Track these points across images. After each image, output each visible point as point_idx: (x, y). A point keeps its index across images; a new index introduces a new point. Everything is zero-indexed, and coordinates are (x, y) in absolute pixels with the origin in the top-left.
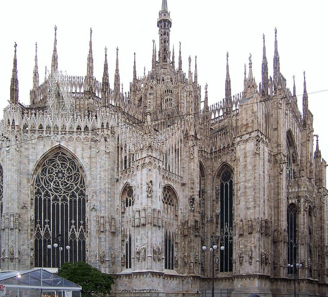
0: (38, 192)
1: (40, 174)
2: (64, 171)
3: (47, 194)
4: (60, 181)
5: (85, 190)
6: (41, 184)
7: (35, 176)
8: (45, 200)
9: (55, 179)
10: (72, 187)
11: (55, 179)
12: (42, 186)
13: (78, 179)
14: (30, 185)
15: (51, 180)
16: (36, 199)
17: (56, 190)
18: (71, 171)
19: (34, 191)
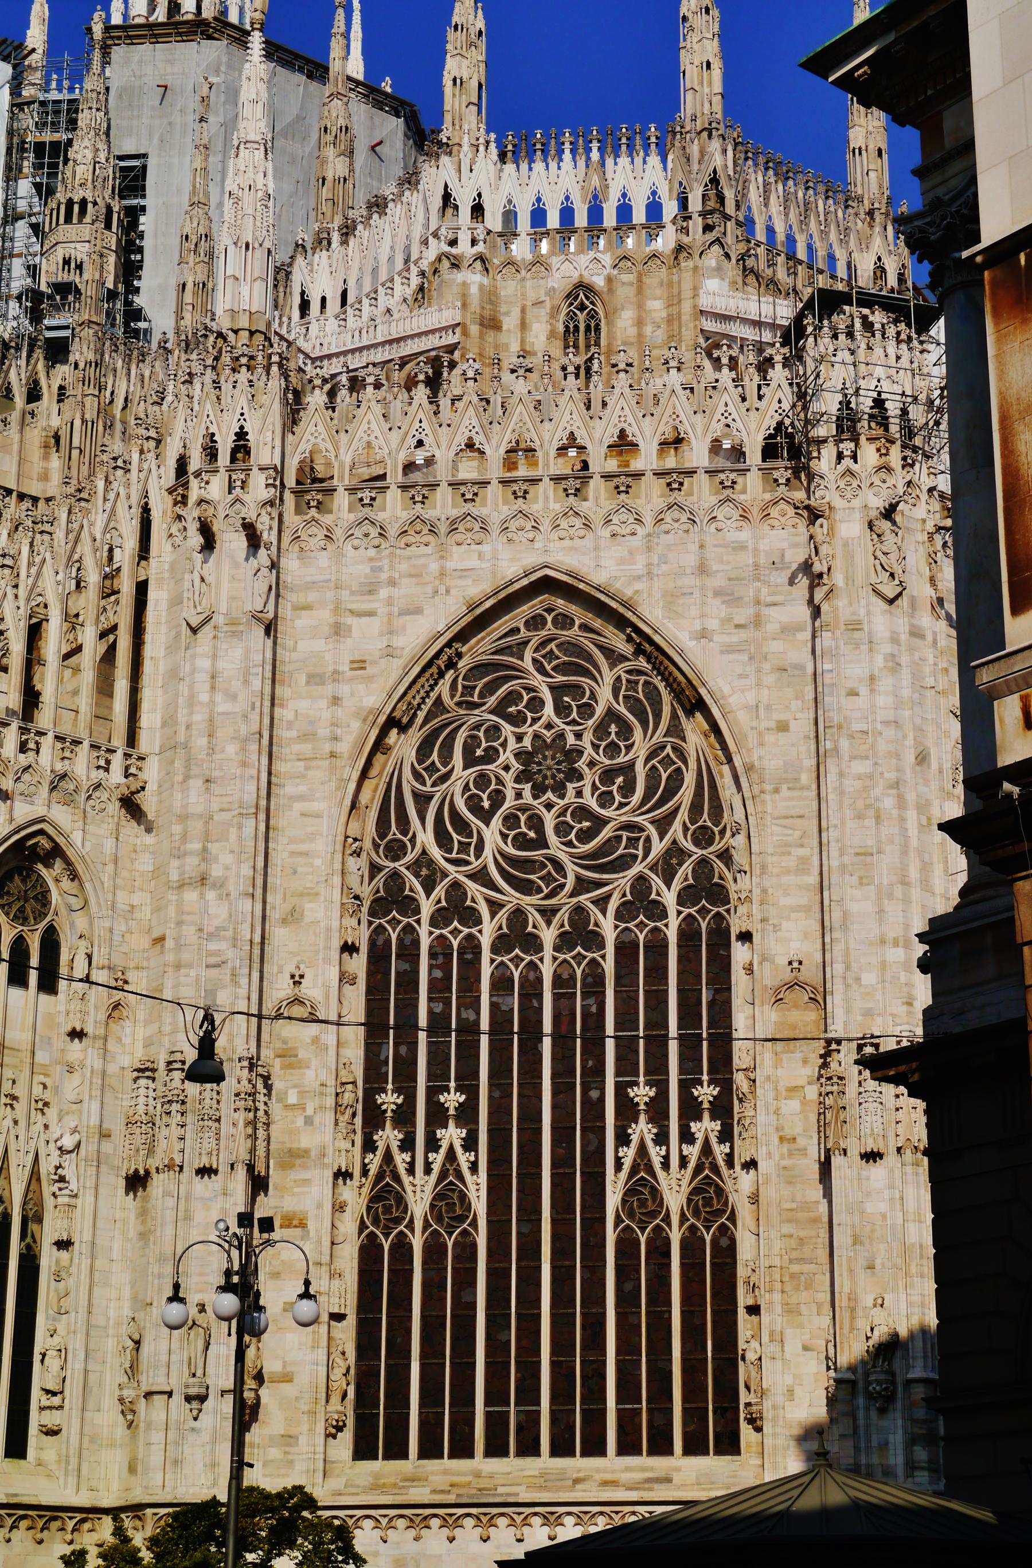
1: (407, 773)
3: (457, 909)
8: (440, 950)
10: (632, 842)
11: (510, 794)
12: (424, 852)
15: (486, 804)
17: (520, 873)
18: (625, 731)
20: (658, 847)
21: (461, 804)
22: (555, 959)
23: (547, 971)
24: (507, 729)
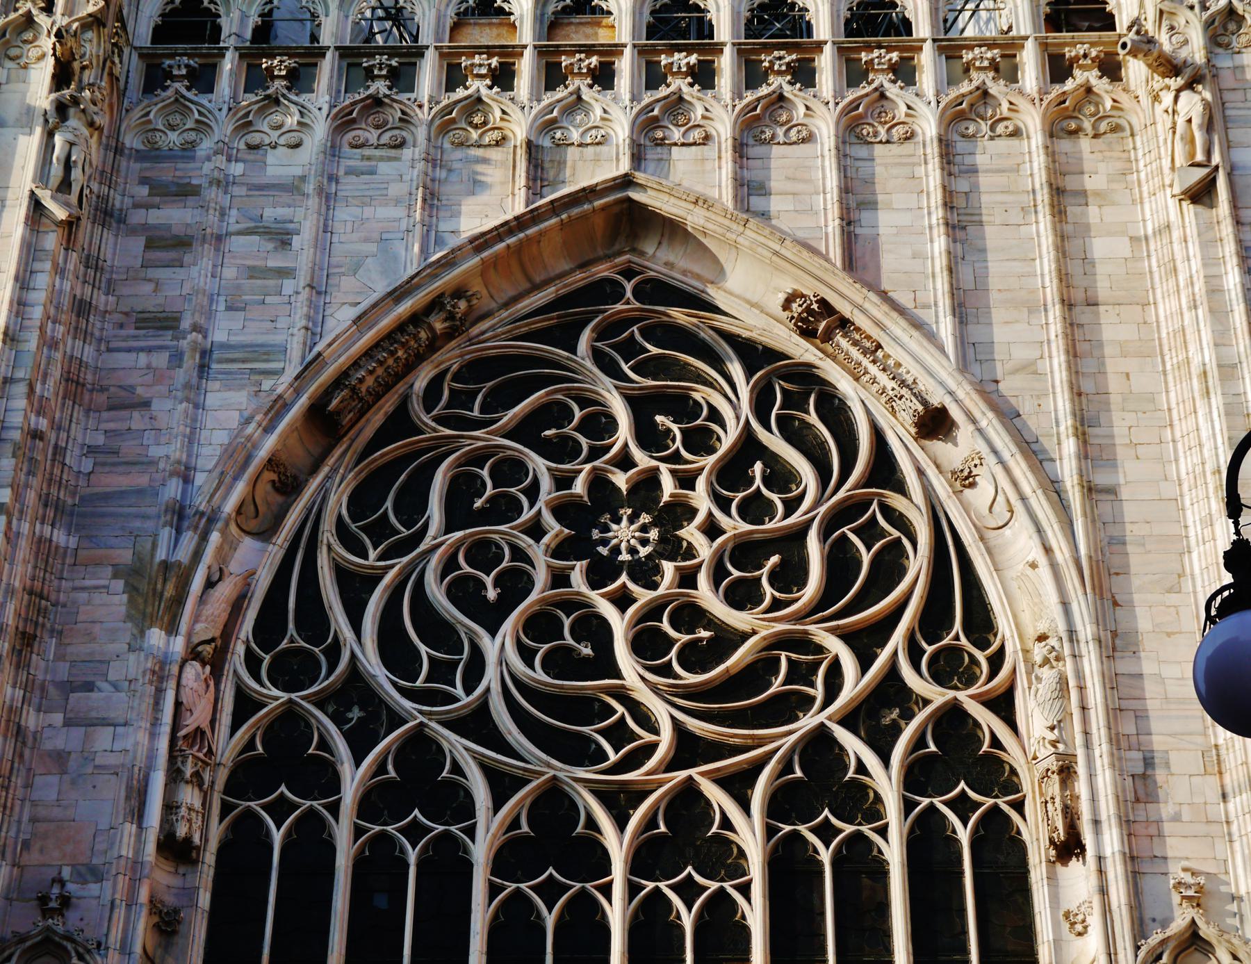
0: (285, 760)
2: (686, 481)
4: (622, 601)
5: (1003, 704)
6: (334, 652)
7: (258, 561)
8: (377, 866)
9: (541, 577)
11: (541, 577)
13: (889, 567)
14: (178, 645)
15: (492, 594)
16: (244, 844)
19: (227, 746)
20: (853, 685)
21: (436, 592)
22: (633, 889)
23: (617, 914)
24: (539, 464)
